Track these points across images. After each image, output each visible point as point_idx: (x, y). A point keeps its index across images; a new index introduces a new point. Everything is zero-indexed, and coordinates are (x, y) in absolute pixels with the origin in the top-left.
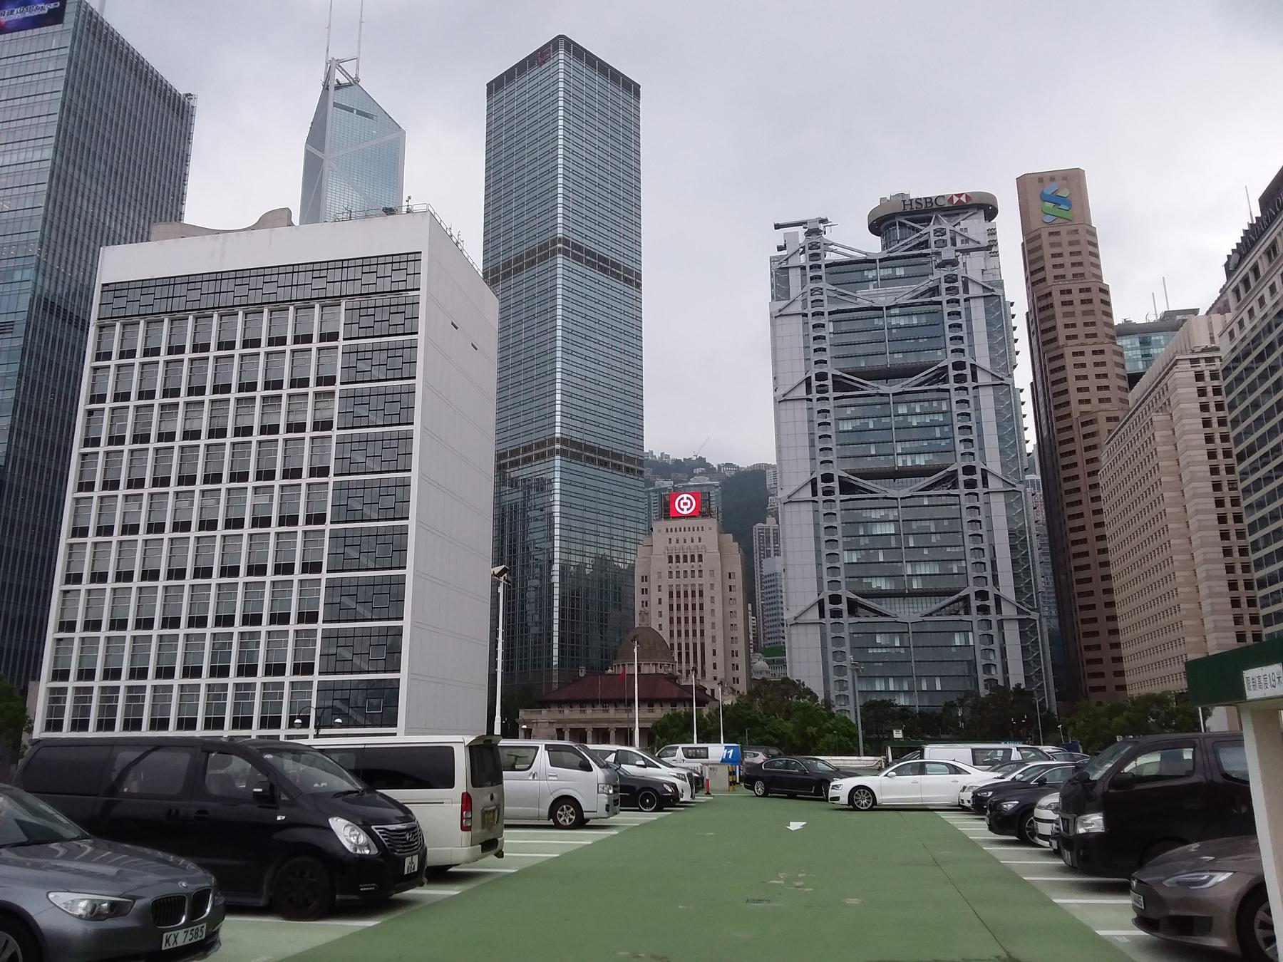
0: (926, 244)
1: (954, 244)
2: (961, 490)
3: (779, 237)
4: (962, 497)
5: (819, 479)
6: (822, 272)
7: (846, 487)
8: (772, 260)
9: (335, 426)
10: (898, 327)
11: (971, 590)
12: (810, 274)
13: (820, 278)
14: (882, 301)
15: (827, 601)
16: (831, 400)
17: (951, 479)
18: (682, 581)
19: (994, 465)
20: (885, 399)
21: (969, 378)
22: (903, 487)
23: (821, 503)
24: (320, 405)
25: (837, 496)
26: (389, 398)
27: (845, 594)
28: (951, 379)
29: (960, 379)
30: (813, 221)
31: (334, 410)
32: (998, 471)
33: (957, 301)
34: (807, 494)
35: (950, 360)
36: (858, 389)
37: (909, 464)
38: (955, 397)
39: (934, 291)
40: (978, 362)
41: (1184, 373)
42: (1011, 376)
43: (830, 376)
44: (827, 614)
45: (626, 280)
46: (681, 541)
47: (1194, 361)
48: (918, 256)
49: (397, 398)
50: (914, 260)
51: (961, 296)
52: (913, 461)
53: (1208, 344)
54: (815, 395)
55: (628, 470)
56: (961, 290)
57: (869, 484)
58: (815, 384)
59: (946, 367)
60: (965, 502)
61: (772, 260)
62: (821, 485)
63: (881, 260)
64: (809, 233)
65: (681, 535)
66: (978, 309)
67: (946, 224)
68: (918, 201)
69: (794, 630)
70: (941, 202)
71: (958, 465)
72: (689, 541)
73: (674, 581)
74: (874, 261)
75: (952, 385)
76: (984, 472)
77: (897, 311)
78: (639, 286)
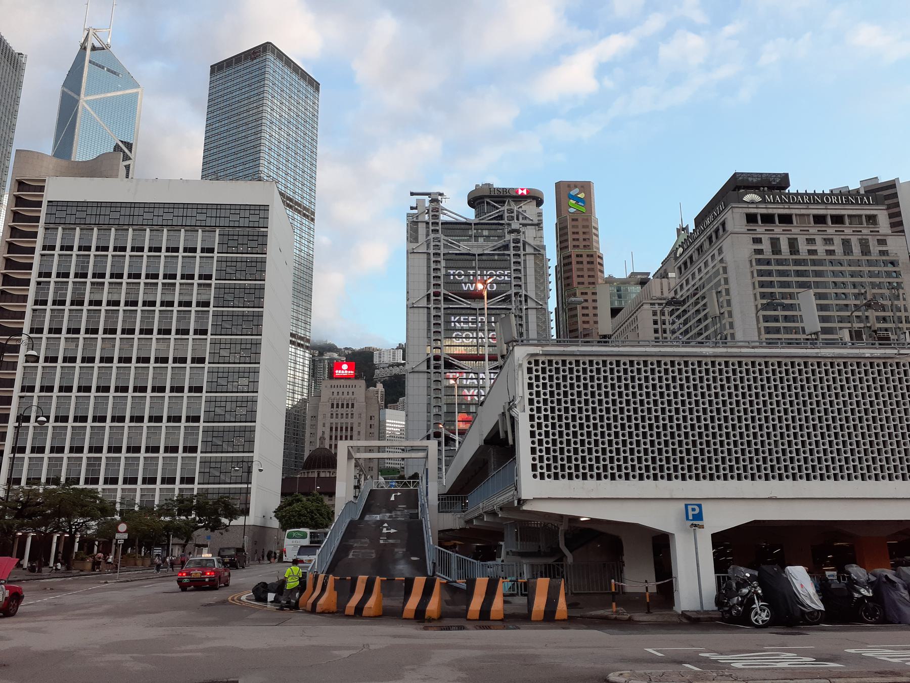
0: (501, 217)
1: (518, 219)
5: (432, 359)
8: (408, 215)
12: (431, 228)
13: (438, 231)
18: (339, 421)
20: (474, 312)
23: (432, 374)
24: (200, 291)
25: (442, 370)
33: (519, 255)
34: (424, 367)
35: (513, 291)
39: (506, 247)
40: (529, 294)
42: (546, 303)
45: (304, 215)
46: (340, 393)
47: (652, 304)
48: (498, 223)
50: (494, 227)
51: (522, 252)
53: (658, 294)
54: (432, 305)
55: (299, 345)
57: (464, 363)
61: (408, 215)
63: (475, 224)
64: (432, 201)
65: (341, 390)
66: (530, 261)
68: (498, 189)
72: (346, 393)
73: (334, 420)
74: (470, 224)
78: (313, 220)
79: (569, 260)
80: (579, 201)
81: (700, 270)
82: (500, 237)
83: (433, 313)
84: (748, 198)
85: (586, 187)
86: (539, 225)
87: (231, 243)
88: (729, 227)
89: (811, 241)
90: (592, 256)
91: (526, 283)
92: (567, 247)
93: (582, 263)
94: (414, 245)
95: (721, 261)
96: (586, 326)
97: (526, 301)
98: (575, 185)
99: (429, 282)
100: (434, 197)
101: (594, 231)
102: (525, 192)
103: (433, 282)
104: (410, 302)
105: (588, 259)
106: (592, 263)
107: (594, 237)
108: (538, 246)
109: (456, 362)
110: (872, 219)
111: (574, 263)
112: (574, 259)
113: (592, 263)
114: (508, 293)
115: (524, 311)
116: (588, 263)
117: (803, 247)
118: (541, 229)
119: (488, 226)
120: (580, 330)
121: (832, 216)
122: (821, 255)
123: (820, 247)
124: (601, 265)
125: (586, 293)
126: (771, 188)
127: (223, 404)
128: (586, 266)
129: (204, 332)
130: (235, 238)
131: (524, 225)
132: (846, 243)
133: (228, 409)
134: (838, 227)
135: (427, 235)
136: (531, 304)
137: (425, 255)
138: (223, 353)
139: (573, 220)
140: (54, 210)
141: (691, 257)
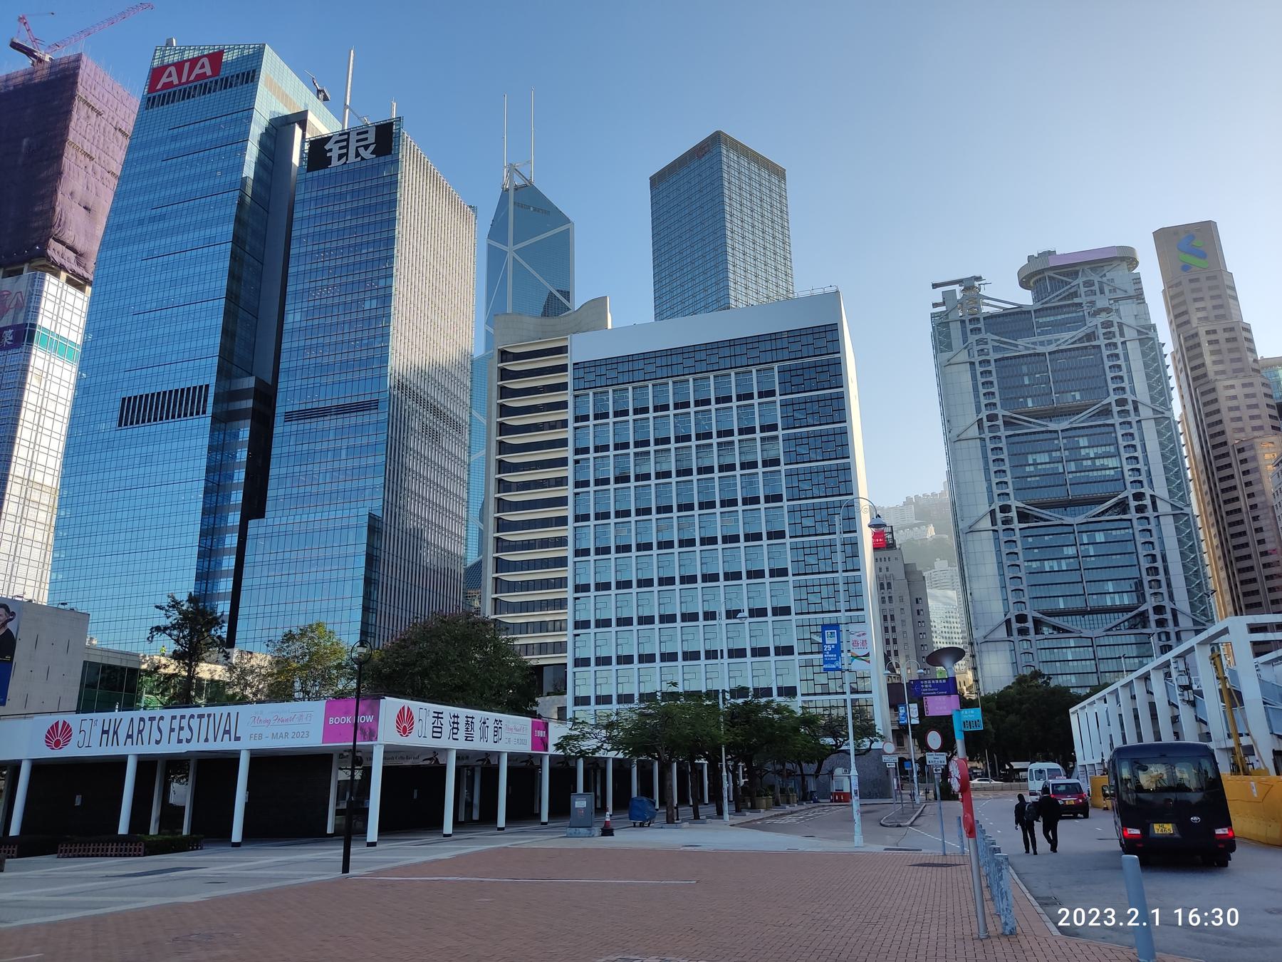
1: (1102, 292)
2: (1133, 515)
3: (937, 296)
4: (1135, 522)
5: (998, 510)
6: (981, 325)
7: (1023, 517)
8: (933, 316)
9: (782, 462)
12: (969, 327)
13: (980, 329)
15: (1013, 620)
16: (1003, 439)
17: (1122, 506)
19: (1161, 490)
20: (1055, 435)
21: (1132, 412)
23: (1001, 532)
25: (1016, 525)
26: (825, 439)
27: (1031, 613)
31: (779, 450)
32: (1166, 496)
33: (1115, 345)
35: (1113, 398)
38: (1120, 432)
39: (1090, 336)
40: (1139, 398)
42: (1170, 409)
44: (1015, 633)
49: (831, 438)
51: (1118, 340)
54: (987, 435)
56: (1117, 334)
57: (1045, 513)
61: (933, 316)
66: (1134, 349)
67: (1096, 278)
69: (984, 647)
74: (1029, 312)
79: (1196, 341)
83: (990, 446)
85: (1208, 230)
86: (1139, 297)
87: (796, 380)
90: (1232, 329)
92: (1188, 322)
93: (1217, 342)
96: (1242, 436)
97: (1136, 409)
101: (1229, 292)
103: (984, 401)
104: (955, 432)
105: (1227, 335)
106: (1234, 339)
107: (1231, 301)
108: (1143, 327)
112: (1204, 339)
114: (1105, 402)
115: (1134, 424)
116: (1228, 340)
120: (1230, 444)
124: (1251, 340)
127: (817, 589)
128: (1224, 346)
129: (778, 498)
130: (800, 372)
131: (1116, 300)
133: (824, 594)
135: (965, 341)
136: (1145, 412)
138: (806, 522)
139: (1191, 281)
140: (581, 373)
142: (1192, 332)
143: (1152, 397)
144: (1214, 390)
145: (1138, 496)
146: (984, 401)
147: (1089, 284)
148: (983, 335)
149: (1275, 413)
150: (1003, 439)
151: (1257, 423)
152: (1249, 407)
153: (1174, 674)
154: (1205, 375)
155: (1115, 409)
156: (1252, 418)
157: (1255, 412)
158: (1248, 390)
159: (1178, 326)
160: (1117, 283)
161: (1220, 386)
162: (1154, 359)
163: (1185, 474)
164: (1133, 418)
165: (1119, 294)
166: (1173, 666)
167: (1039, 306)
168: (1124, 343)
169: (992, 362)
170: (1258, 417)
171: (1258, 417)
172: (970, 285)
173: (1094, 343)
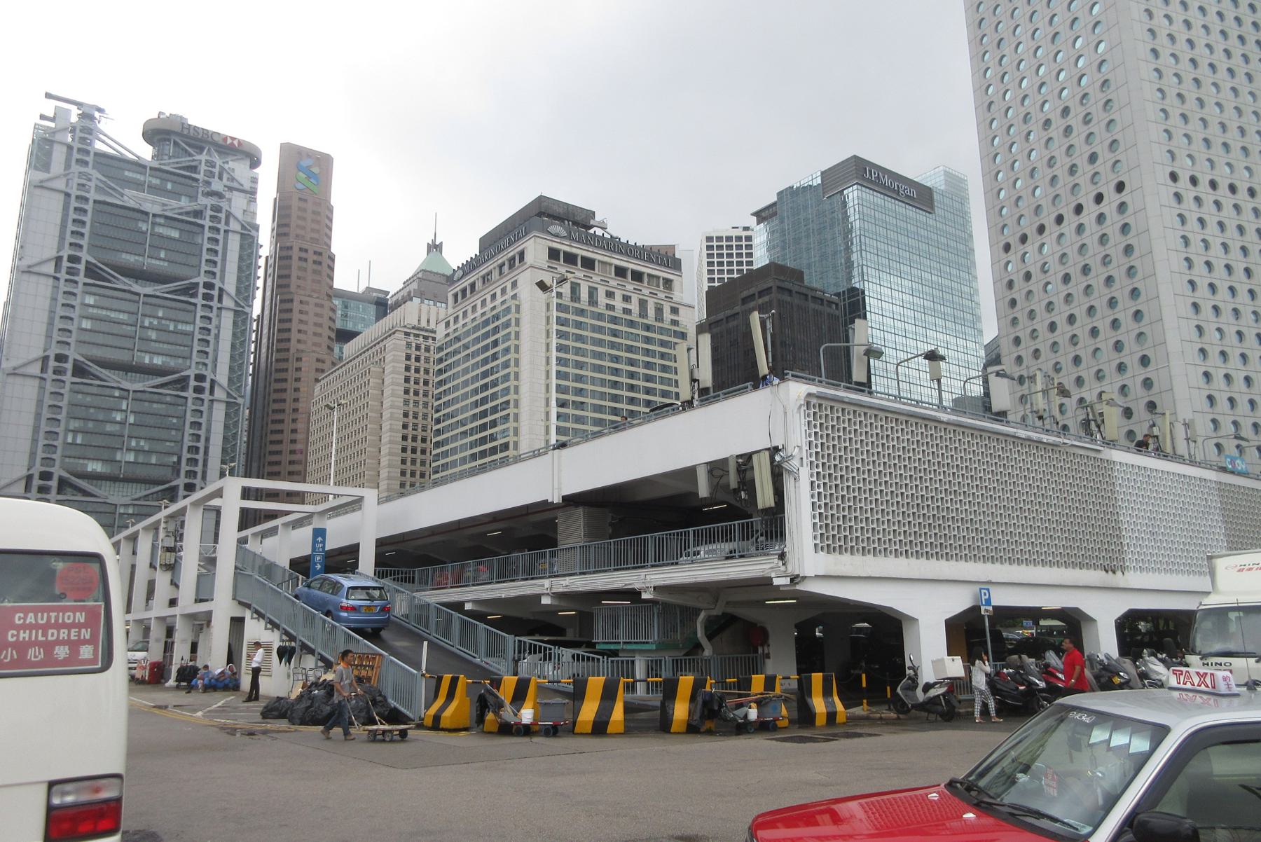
0: (194, 169)
1: (220, 178)
2: (190, 394)
3: (49, 108)
4: (190, 401)
6: (90, 159)
7: (79, 370)
8: (36, 127)
10: (161, 236)
11: (181, 481)
12: (76, 156)
13: (86, 163)
14: (147, 207)
15: (36, 476)
16: (80, 285)
17: (182, 383)
19: (222, 377)
21: (216, 299)
22: (135, 381)
23: (49, 383)
25: (68, 378)
27: (57, 471)
28: (200, 296)
29: (207, 297)
30: (88, 105)
33: (218, 230)
34: (35, 369)
35: (201, 279)
36: (109, 281)
37: (147, 361)
39: (198, 214)
40: (226, 287)
41: (398, 341)
42: (251, 306)
43: (83, 262)
47: (407, 334)
50: (182, 180)
51: (222, 227)
52: (151, 359)
53: (415, 323)
54: (63, 275)
57: (104, 373)
58: (66, 265)
59: (197, 284)
60: (190, 406)
62: (52, 364)
63: (151, 169)
66: (234, 243)
70: (216, 138)
71: (191, 373)
74: (144, 167)
75: (199, 301)
76: (213, 382)
77: (162, 221)
79: (290, 253)
80: (310, 175)
81: (484, 303)
82: (193, 198)
84: (556, 228)
86: (252, 194)
88: (529, 258)
89: (610, 295)
90: (320, 254)
91: (223, 271)
93: (306, 260)
94: (42, 176)
95: (514, 297)
98: (310, 154)
99: (62, 238)
100: (87, 110)
102: (236, 143)
104: (26, 262)
105: (315, 258)
108: (249, 224)
109: (95, 369)
110: (668, 283)
111: (295, 258)
112: (295, 254)
113: (320, 263)
115: (215, 310)
116: (315, 262)
117: (602, 300)
118: (254, 200)
119: (175, 178)
121: (633, 272)
122: (618, 313)
123: (618, 303)
124: (332, 269)
125: (307, 303)
126: (575, 223)
132: (643, 304)
134: (636, 284)
135: (68, 166)
136: (228, 302)
137: (62, 197)
141: (473, 285)
142: (288, 244)
143: (238, 291)
144: (292, 301)
145: (201, 378)
146: (69, 239)
147: (211, 164)
148: (89, 170)
149: (333, 336)
150: (80, 285)
151: (317, 339)
152: (316, 324)
153: (162, 534)
154: (288, 286)
155: (202, 290)
156: (315, 334)
157: (319, 330)
158: (318, 310)
159: (278, 235)
160: (237, 175)
161: (297, 299)
162: (250, 255)
163: (247, 368)
164: (215, 304)
165: (235, 185)
166: (163, 525)
167: (156, 164)
168: (226, 232)
169: (91, 202)
170: (320, 335)
171: (320, 335)
172: (88, 115)
173: (199, 221)
